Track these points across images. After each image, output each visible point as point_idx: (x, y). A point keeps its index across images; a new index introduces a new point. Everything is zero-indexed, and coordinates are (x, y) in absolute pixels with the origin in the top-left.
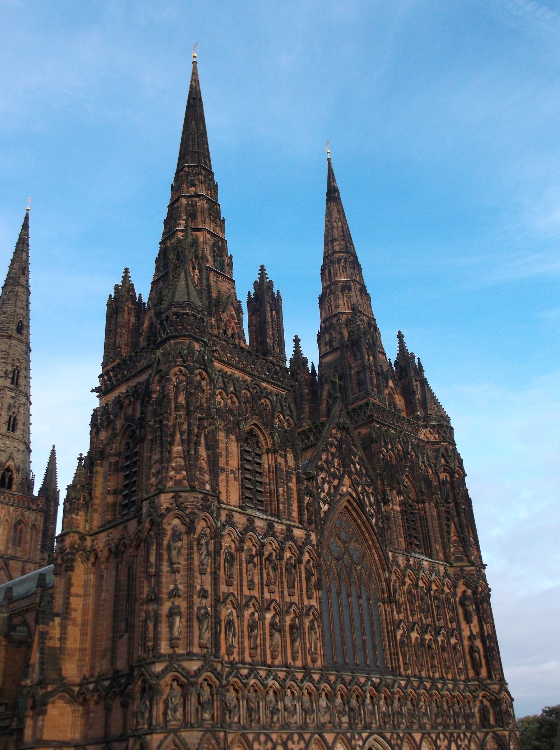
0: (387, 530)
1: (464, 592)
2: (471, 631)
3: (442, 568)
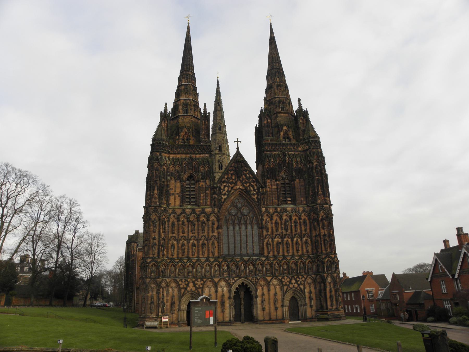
2: (316, 233)
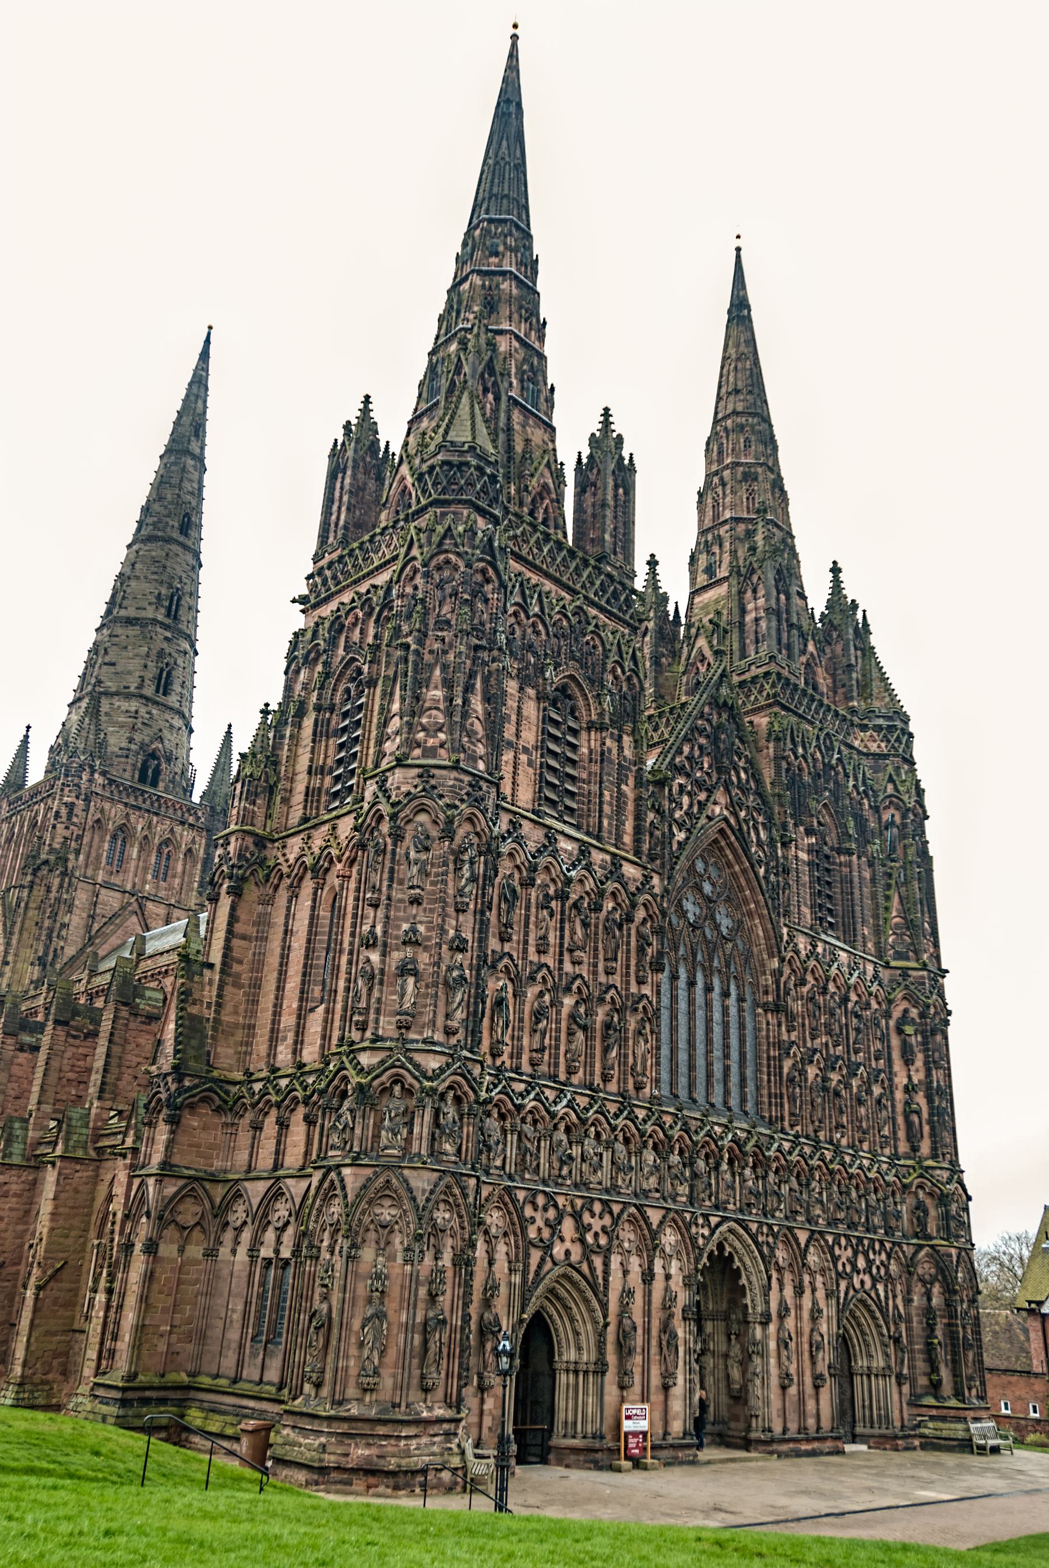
0: (784, 889)
1: (906, 1011)
3: (870, 968)
